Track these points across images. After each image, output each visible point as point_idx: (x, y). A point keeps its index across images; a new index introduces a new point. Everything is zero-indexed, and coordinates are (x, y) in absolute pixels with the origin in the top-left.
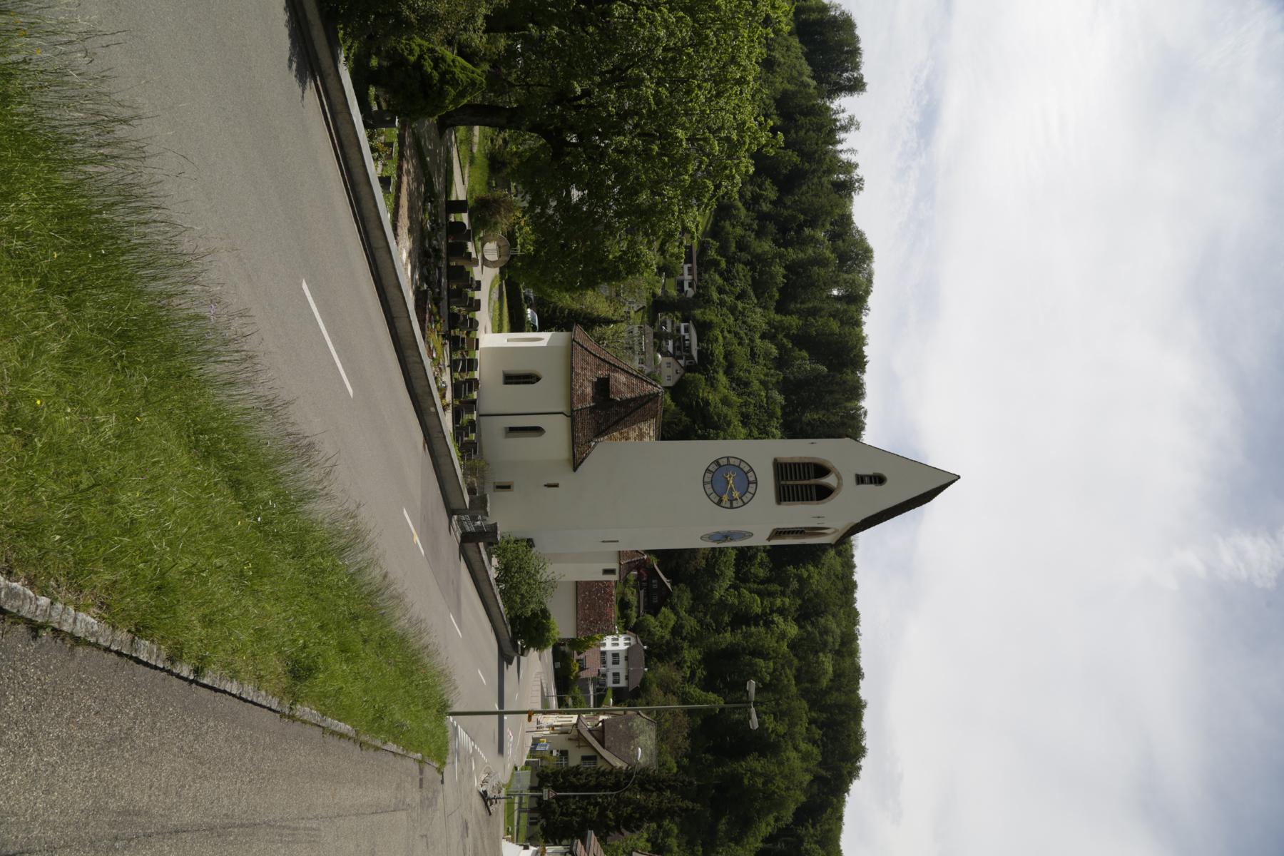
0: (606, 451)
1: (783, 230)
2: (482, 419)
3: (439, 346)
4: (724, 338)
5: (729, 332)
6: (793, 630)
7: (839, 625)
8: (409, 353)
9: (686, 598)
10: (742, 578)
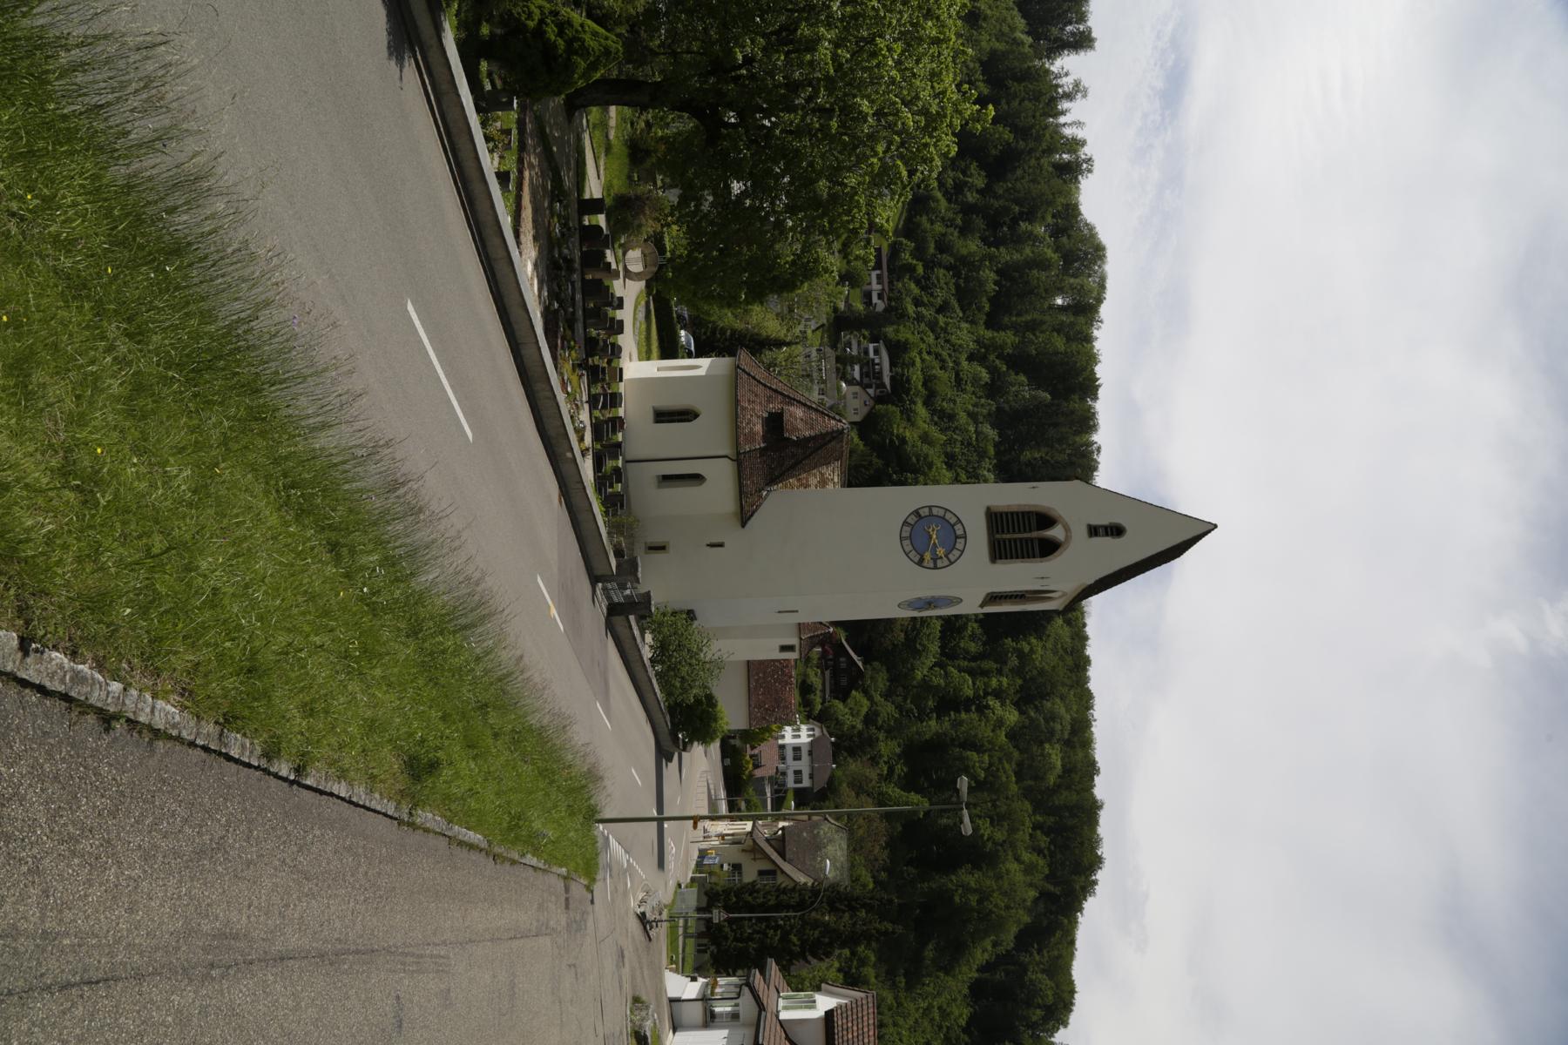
0: (780, 502)
1: (994, 222)
2: (630, 466)
3: (574, 378)
4: (923, 360)
5: (929, 353)
6: (1012, 717)
7: (1068, 710)
8: (538, 386)
9: (882, 680)
10: (949, 653)
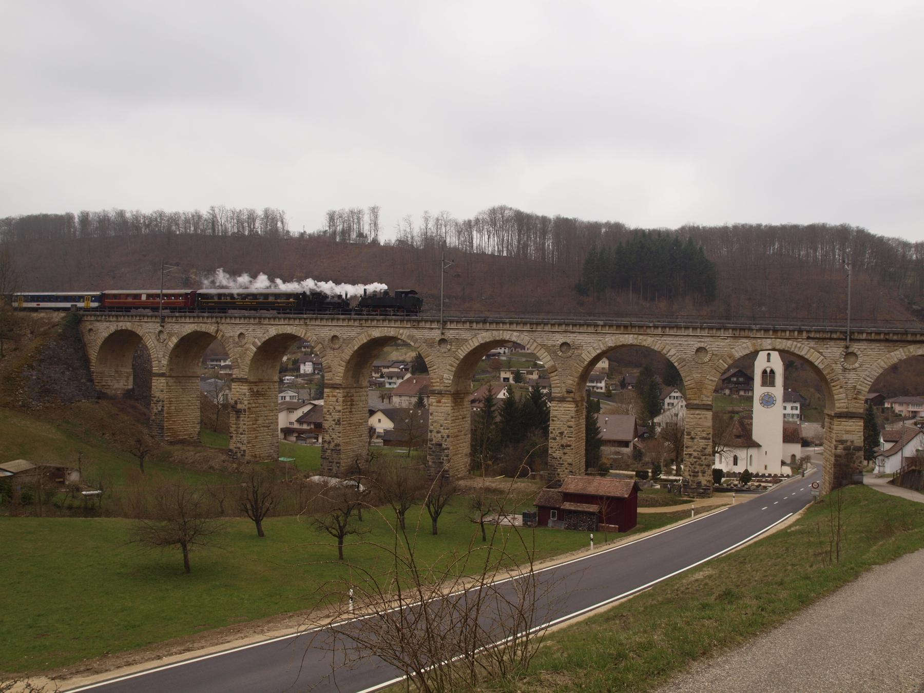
0: (756, 436)
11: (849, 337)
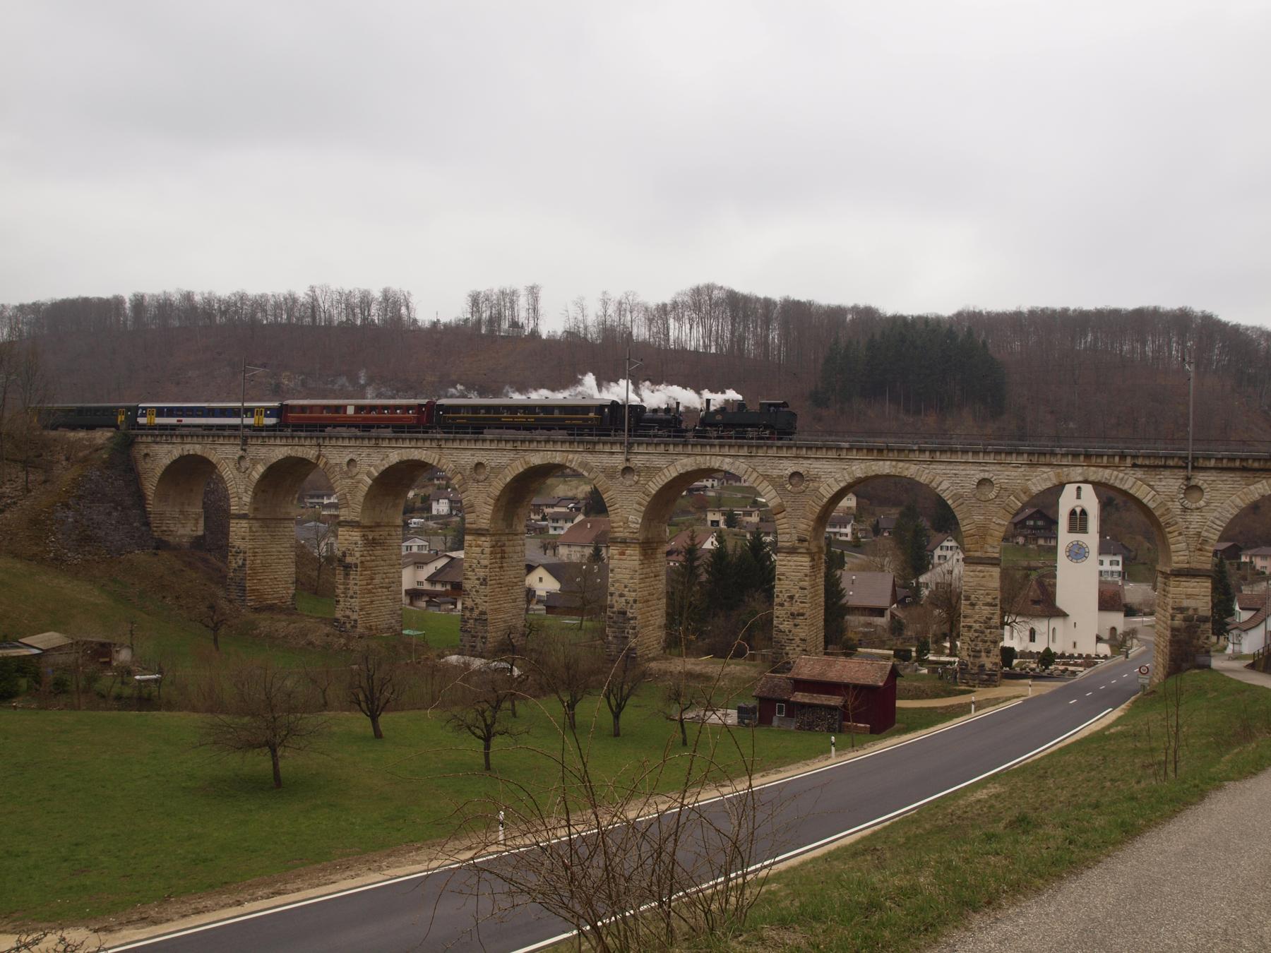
0: (1060, 603)
11: (1191, 465)
